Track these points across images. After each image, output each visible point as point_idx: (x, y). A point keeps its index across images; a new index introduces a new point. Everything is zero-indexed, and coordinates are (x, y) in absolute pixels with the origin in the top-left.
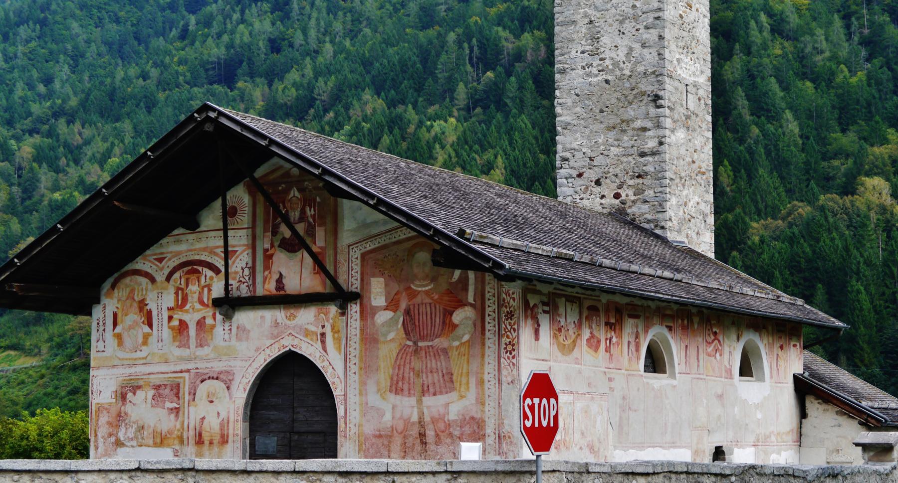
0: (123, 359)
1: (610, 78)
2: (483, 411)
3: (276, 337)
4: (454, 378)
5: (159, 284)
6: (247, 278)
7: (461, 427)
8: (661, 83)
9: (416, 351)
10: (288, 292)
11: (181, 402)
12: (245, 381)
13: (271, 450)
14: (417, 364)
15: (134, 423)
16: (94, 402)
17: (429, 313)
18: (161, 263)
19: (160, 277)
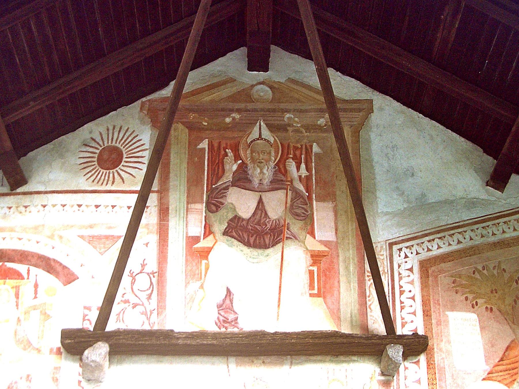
6: (143, 296)
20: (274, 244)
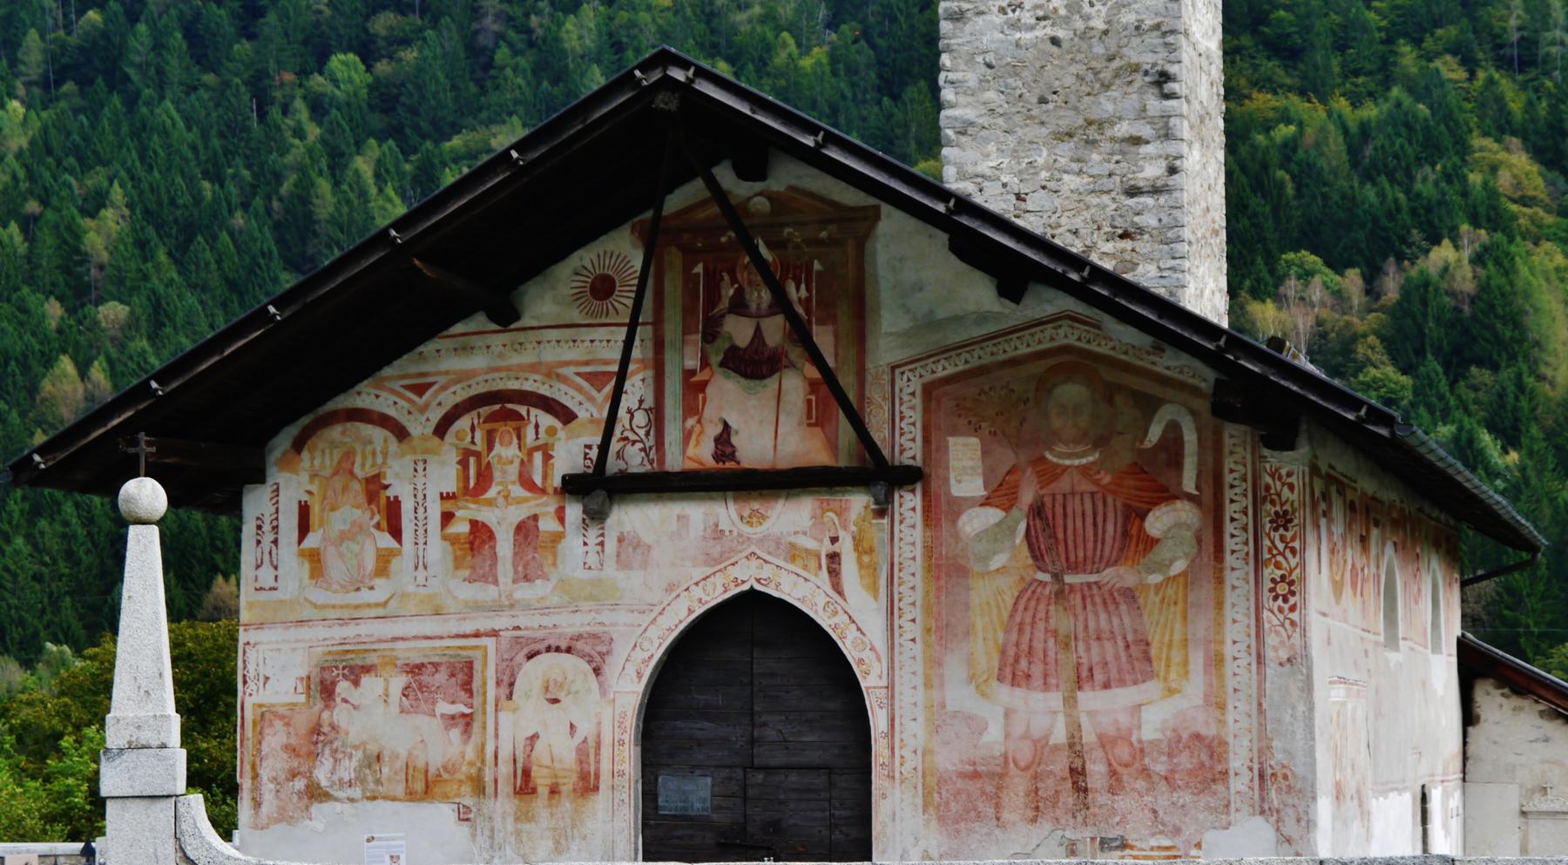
0: (324, 607)
1: (1060, 33)
2: (1222, 723)
3: (717, 562)
4: (1153, 652)
5: (416, 442)
6: (642, 432)
7: (1170, 755)
8: (1171, 48)
9: (1061, 594)
10: (746, 464)
11: (477, 701)
12: (639, 655)
13: (697, 805)
14: (1063, 621)
15: (356, 747)
16: (249, 702)
17: (1089, 512)
18: (420, 394)
19: (420, 427)
20: (770, 374)
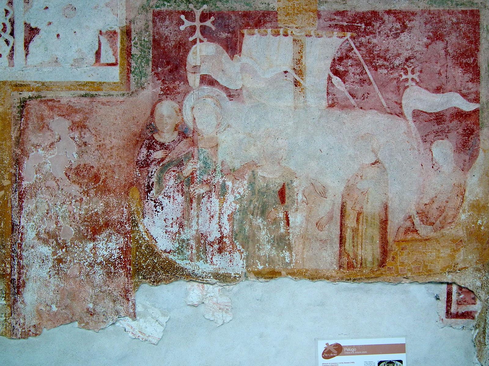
15: (234, 174)
